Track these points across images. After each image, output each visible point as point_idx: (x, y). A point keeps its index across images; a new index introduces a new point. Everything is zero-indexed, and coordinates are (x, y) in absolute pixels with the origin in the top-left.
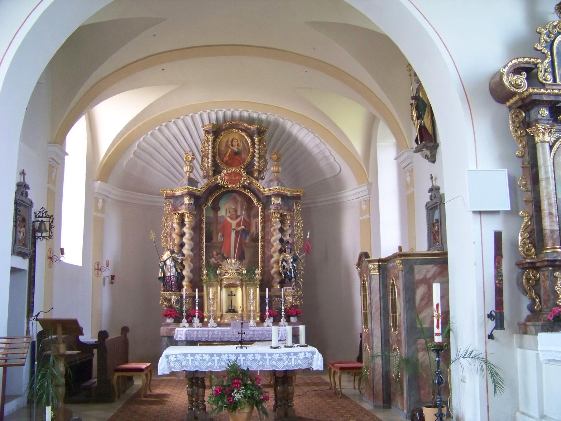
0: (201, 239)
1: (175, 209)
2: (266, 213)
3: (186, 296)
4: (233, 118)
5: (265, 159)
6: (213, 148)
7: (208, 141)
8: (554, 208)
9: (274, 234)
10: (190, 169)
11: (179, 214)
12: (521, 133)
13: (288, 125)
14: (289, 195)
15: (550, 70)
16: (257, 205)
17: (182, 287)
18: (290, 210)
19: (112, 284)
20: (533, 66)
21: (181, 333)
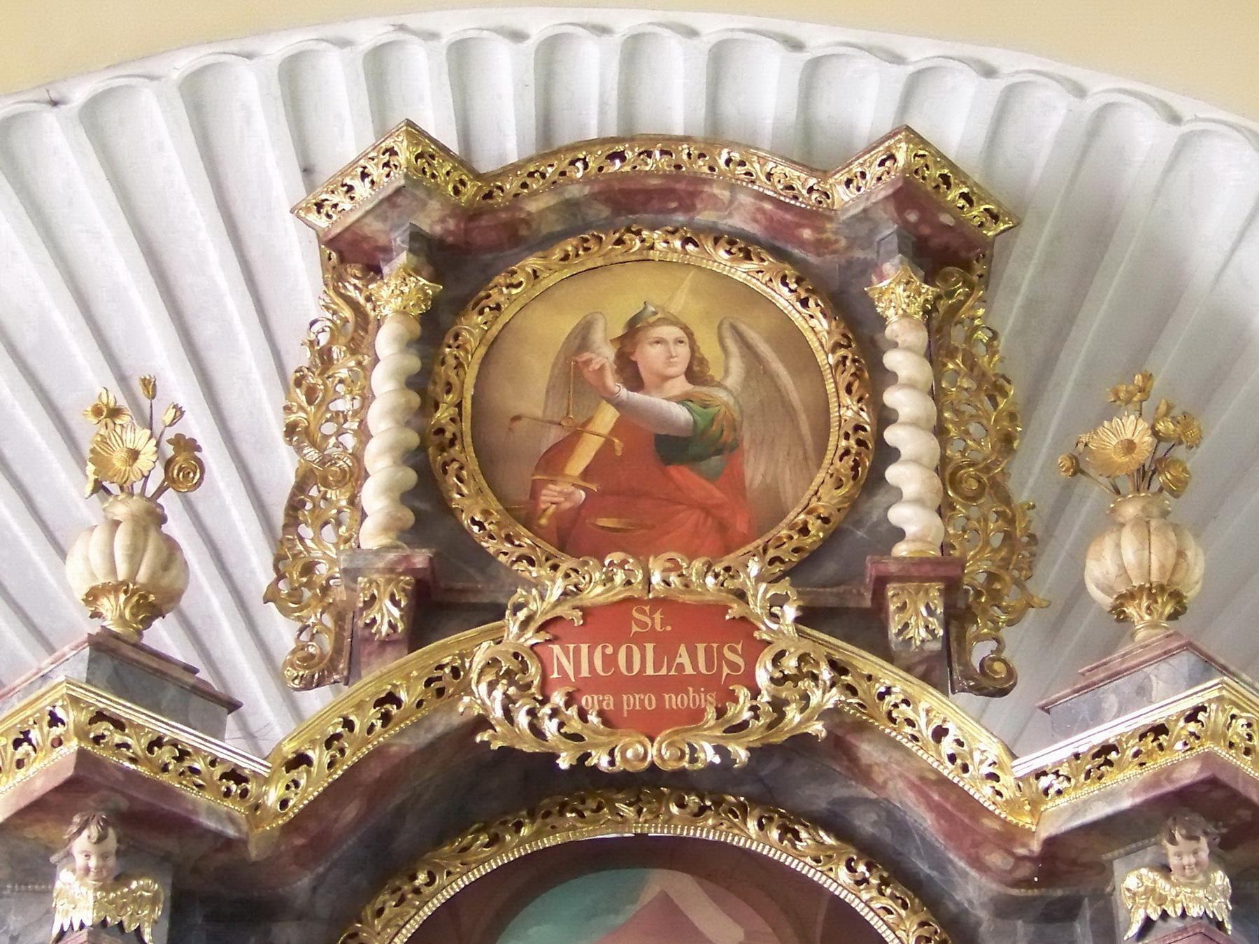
5: (1007, 500)
10: (135, 556)
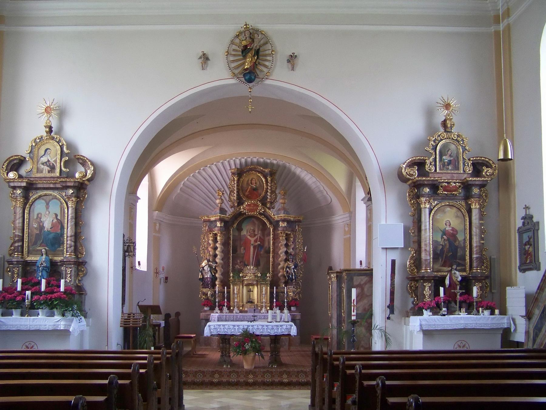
0: (229, 251)
1: (210, 230)
2: (276, 232)
3: (218, 292)
4: (252, 163)
5: (276, 193)
6: (237, 186)
7: (234, 180)
8: (428, 247)
9: (281, 248)
10: (221, 202)
11: (213, 233)
12: (413, 202)
13: (293, 168)
14: (292, 220)
15: (433, 163)
16: (270, 227)
17: (216, 285)
18: (293, 230)
19: (166, 283)
20: (423, 161)
21: (215, 317)
